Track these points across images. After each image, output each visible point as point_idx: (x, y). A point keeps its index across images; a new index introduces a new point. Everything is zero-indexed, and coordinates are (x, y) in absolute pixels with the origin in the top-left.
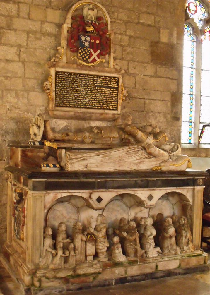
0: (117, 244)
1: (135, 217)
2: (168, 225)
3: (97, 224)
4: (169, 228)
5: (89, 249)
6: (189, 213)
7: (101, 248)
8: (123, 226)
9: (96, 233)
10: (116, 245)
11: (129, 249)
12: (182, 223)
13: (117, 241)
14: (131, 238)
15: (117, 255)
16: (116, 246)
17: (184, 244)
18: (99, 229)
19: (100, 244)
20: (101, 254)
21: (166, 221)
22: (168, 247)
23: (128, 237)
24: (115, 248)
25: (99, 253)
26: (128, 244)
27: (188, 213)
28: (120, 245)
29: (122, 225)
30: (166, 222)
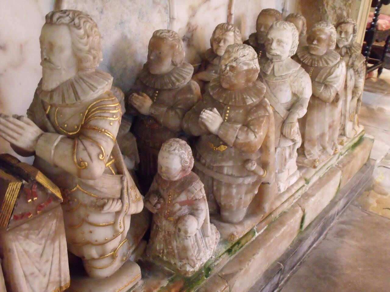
0: (184, 185)
1: (189, 24)
2: (326, 54)
3: (51, 85)
4: (331, 64)
5: (30, 269)
6: (334, 8)
7: (101, 234)
8: (169, 74)
9: (55, 150)
10: (179, 194)
11: (234, 191)
12: (346, 43)
13: (184, 170)
14: (252, 137)
15: (190, 242)
16: (183, 197)
17: (347, 115)
18: (70, 117)
19: (95, 218)
20: (104, 262)
21: (323, 36)
22: (322, 135)
23: (235, 134)
24: (178, 206)
25: (94, 259)
26: (225, 171)
27: (328, 9)
28: (199, 189)
29: (166, 67)
30: (320, 40)
